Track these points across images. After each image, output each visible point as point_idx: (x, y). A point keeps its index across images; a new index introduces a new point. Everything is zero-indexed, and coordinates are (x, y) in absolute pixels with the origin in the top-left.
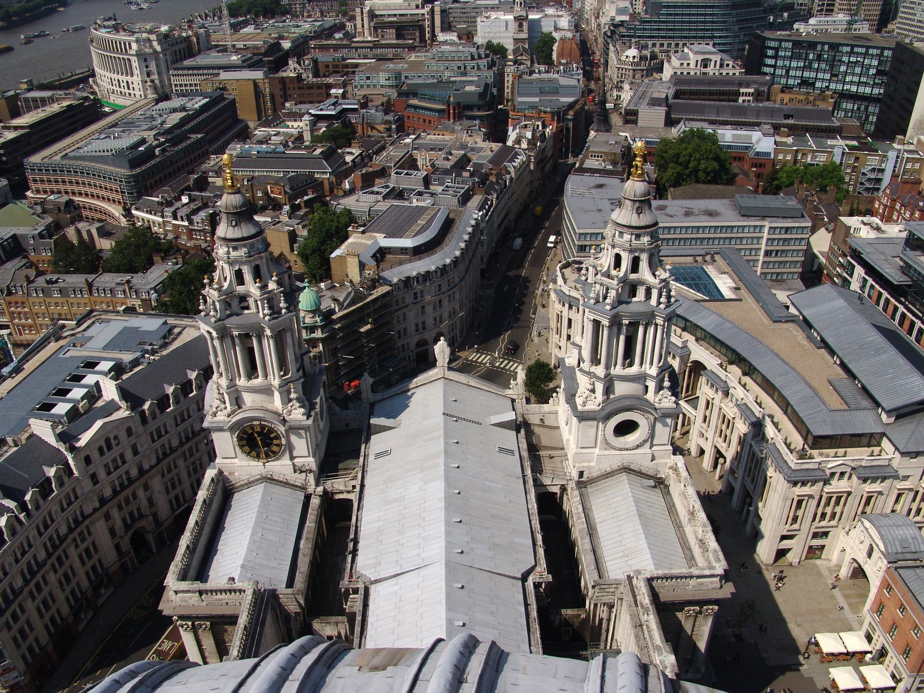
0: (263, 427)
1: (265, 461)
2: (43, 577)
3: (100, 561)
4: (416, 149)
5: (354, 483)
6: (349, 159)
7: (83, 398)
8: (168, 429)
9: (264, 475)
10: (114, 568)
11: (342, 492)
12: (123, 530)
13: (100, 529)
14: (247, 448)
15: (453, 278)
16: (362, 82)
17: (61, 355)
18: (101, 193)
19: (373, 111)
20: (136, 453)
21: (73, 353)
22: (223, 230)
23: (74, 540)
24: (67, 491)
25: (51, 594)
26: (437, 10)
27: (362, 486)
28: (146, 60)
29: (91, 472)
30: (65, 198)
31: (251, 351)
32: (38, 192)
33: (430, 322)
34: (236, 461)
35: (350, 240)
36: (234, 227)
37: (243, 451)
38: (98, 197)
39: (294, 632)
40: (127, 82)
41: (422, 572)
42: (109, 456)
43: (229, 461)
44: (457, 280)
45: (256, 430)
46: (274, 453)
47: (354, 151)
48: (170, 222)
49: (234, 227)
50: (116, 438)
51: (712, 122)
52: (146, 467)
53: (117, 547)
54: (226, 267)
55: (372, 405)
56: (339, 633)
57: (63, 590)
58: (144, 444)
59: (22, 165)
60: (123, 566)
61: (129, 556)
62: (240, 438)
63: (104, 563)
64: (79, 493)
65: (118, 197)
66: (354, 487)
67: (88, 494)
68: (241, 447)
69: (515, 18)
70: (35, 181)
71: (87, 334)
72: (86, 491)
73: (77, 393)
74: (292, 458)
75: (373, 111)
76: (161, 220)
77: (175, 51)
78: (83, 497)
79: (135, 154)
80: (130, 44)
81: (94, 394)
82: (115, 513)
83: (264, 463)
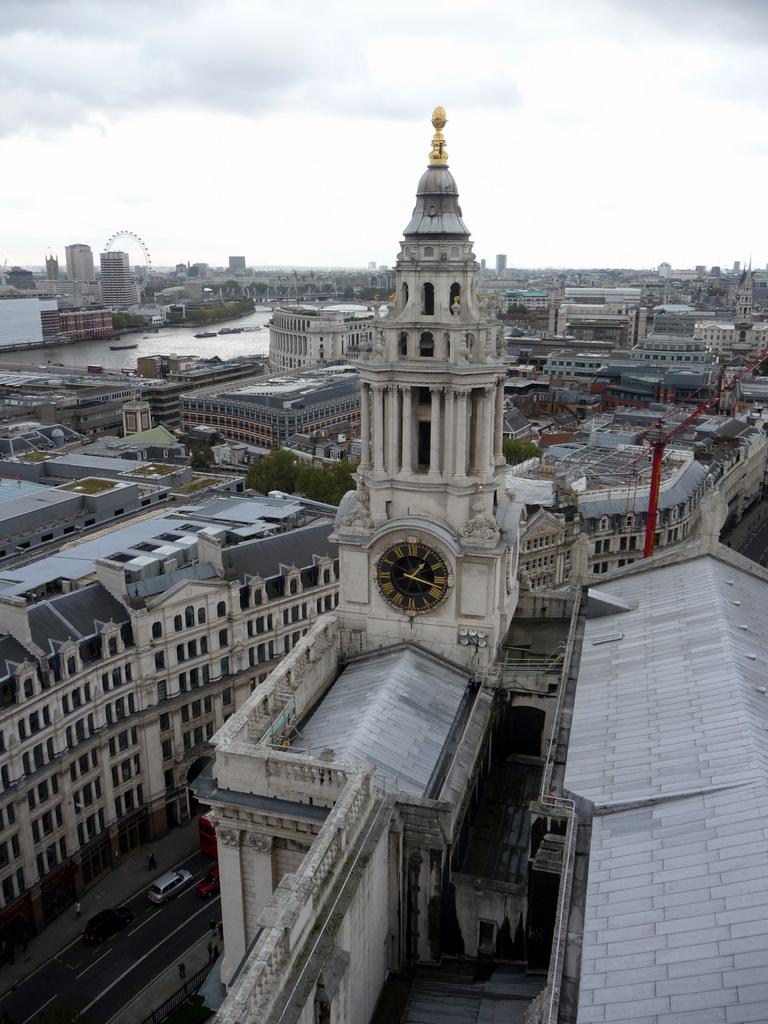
0: (422, 548)
1: (414, 613)
2: (54, 778)
3: (139, 788)
5: (552, 680)
7: (173, 556)
8: (274, 624)
9: (408, 638)
10: (157, 806)
11: (530, 695)
12: (182, 749)
13: (152, 736)
14: (389, 586)
15: (676, 529)
16: (554, 368)
19: (567, 389)
20: (223, 641)
23: (112, 741)
24: (119, 664)
25: (58, 809)
26: (643, 316)
27: (572, 680)
28: (322, 339)
29: (158, 649)
30: (213, 430)
31: (424, 430)
34: (365, 610)
36: (432, 217)
37: (383, 592)
38: (247, 438)
39: (420, 895)
40: (299, 361)
41: (709, 801)
42: (187, 635)
43: (356, 608)
45: (410, 554)
46: (431, 600)
47: (540, 423)
48: (320, 460)
49: (432, 217)
50: (202, 611)
52: (234, 669)
53: (168, 776)
56: (506, 922)
57: (78, 810)
58: (239, 635)
59: (177, 398)
60: (170, 808)
61: (181, 796)
62: (382, 566)
63: (146, 793)
64: (134, 674)
65: (270, 439)
66: (553, 688)
67: (147, 679)
68: (381, 581)
69: (736, 327)
70: (186, 417)
72: (144, 675)
74: (459, 615)
75: (567, 389)
76: (311, 456)
77: (353, 336)
78: (139, 682)
80: (309, 323)
82: (176, 722)
83: (412, 618)
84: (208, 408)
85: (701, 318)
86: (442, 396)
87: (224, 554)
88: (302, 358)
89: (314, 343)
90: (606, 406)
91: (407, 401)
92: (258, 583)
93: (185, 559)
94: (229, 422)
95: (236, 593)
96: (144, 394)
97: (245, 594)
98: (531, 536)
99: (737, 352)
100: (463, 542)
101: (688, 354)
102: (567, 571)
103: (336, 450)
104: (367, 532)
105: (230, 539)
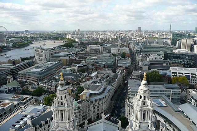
4: (98, 74)
6: (84, 75)
7: (23, 124)
17: (19, 114)
18: (34, 80)
21: (23, 113)
22: (59, 88)
30: (26, 80)
31: (62, 114)
32: (20, 79)
33: (100, 109)
35: (84, 91)
44: (106, 100)
51: (158, 69)
54: (59, 96)
55: (87, 127)
59: (18, 73)
71: (26, 109)
73: (22, 122)
79: (41, 72)
81: (25, 123)
84: (24, 75)
85: (112, 47)
86: (64, 111)
87: (32, 121)
88: (42, 58)
89: (44, 55)
90: (96, 69)
91: (59, 112)
92: (38, 126)
93: (25, 123)
94: (28, 77)
95: (34, 129)
96: (10, 70)
97: (36, 128)
98: (82, 106)
99: (118, 53)
100: (69, 130)
101: (110, 57)
102: (89, 110)
103: (50, 84)
104: (55, 130)
105: (32, 118)
